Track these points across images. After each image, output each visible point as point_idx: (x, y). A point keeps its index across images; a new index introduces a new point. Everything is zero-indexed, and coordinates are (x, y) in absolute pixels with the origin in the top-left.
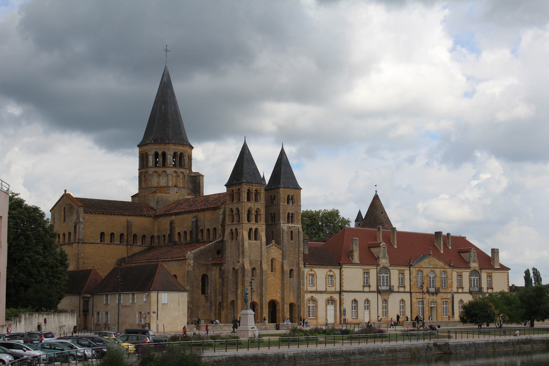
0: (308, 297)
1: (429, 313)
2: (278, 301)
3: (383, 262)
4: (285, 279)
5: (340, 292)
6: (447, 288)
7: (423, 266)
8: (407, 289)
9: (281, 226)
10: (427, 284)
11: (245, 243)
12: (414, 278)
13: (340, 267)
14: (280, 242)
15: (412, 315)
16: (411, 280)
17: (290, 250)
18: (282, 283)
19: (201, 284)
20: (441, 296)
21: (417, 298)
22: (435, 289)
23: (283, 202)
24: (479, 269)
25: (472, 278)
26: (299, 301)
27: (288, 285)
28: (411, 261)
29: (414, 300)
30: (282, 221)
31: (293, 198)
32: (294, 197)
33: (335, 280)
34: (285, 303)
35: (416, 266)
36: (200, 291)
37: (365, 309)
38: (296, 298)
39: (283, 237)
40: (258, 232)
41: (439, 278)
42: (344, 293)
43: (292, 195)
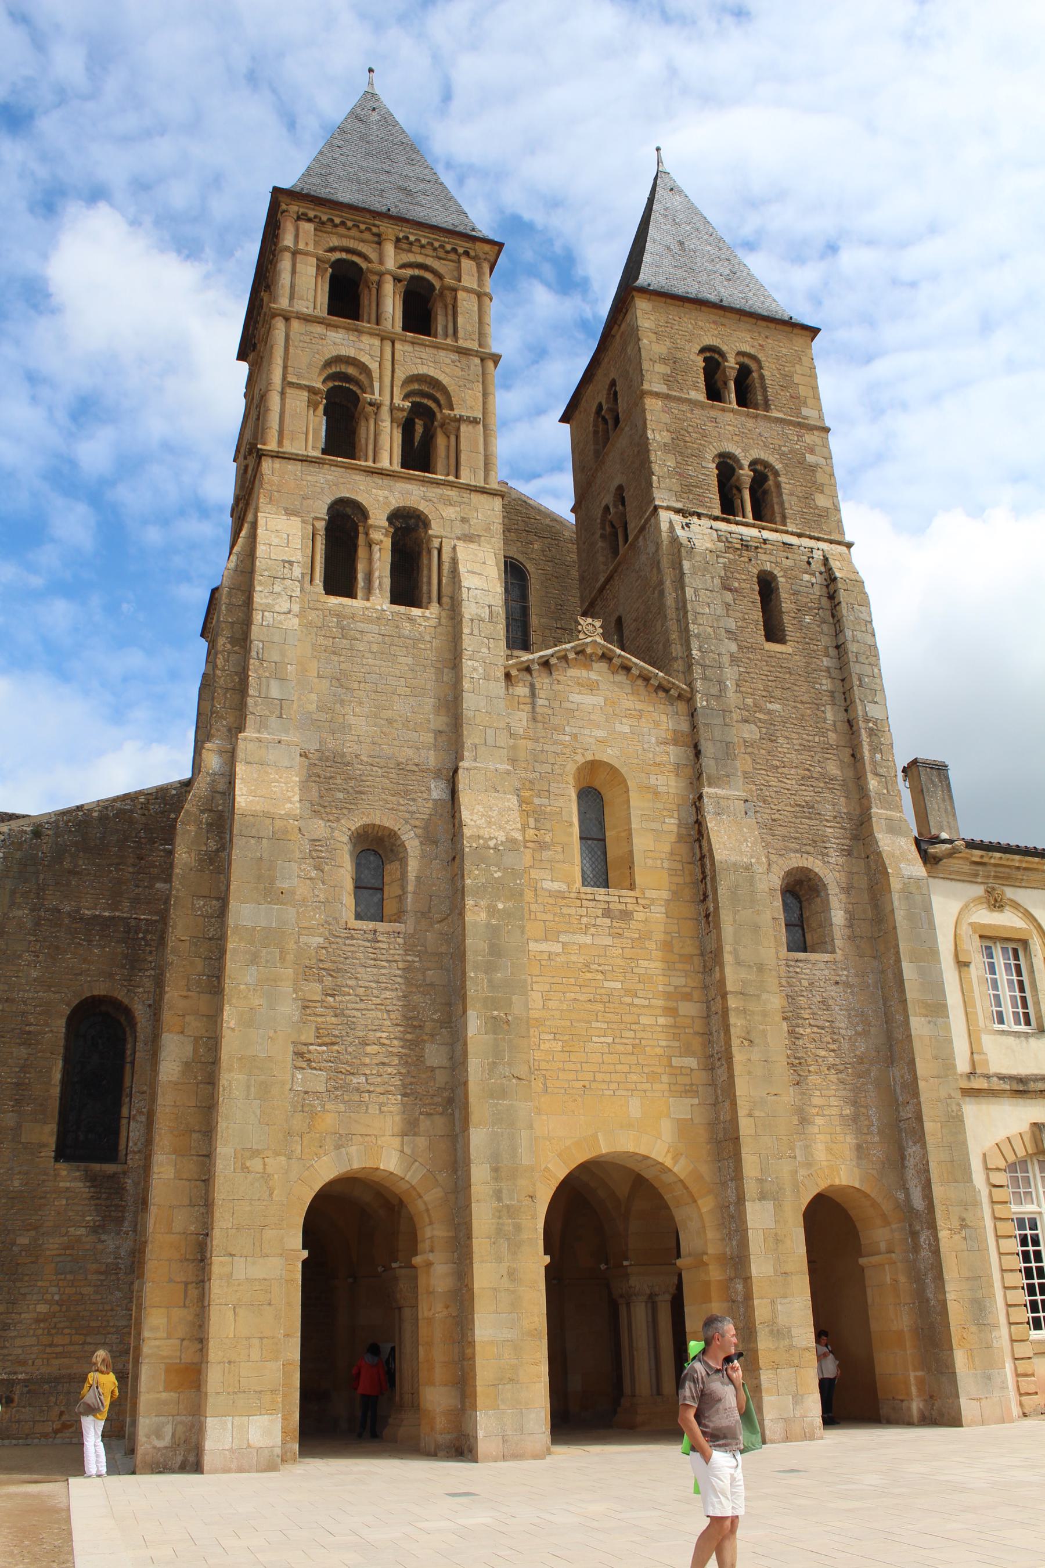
0: (1001, 1135)
2: (680, 1168)
4: (727, 948)
9: (664, 526)
11: (258, 599)
14: (667, 644)
17: (769, 712)
18: (705, 987)
19: (57, 1076)
23: (667, 380)
26: (910, 1173)
27: (775, 1002)
30: (661, 498)
31: (755, 375)
32: (761, 368)
34: (750, 1188)
36: (47, 1134)
38: (876, 1139)
39: (682, 605)
40: (429, 539)
43: (746, 361)
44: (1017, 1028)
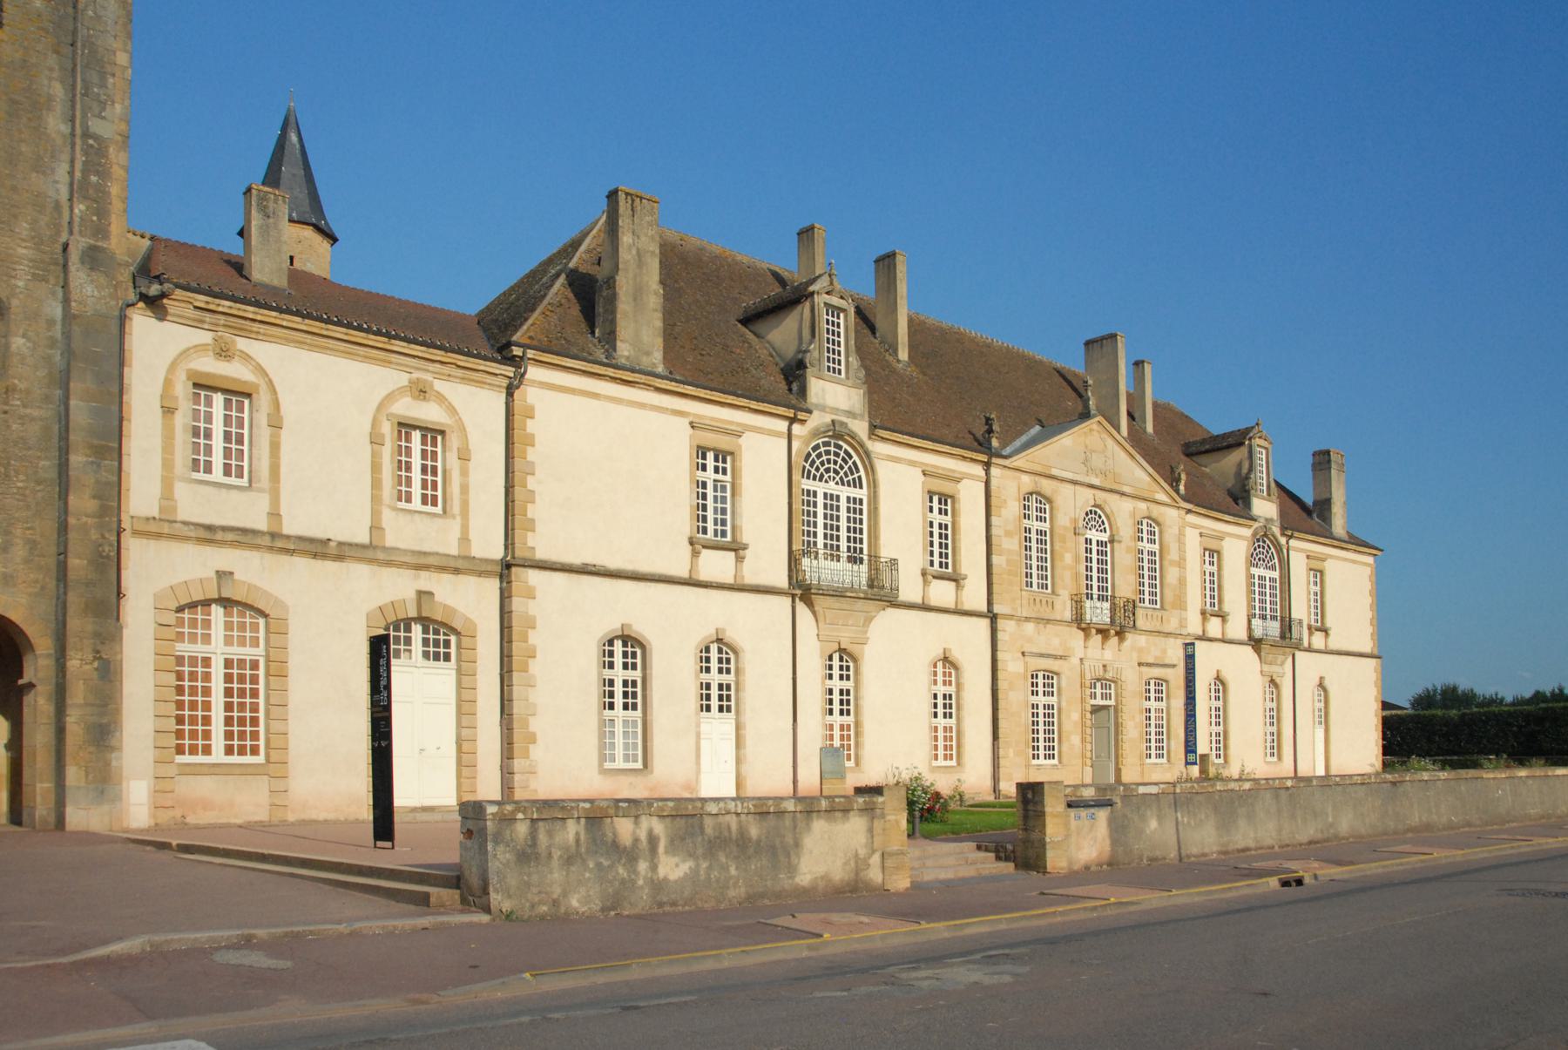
1: (1083, 741)
3: (830, 401)
5: (506, 569)
6: (1162, 608)
7: (1055, 472)
8: (975, 595)
10: (1077, 575)
12: (1008, 534)
13: (509, 371)
15: (1001, 752)
16: (994, 541)
20: (1140, 650)
21: (1023, 654)
22: (1113, 610)
24: (1283, 534)
25: (1255, 571)
28: (996, 427)
29: (1012, 665)
33: (464, 473)
35: (1018, 461)
37: (708, 709)
41: (1128, 550)
42: (534, 577)
44: (227, 480)
